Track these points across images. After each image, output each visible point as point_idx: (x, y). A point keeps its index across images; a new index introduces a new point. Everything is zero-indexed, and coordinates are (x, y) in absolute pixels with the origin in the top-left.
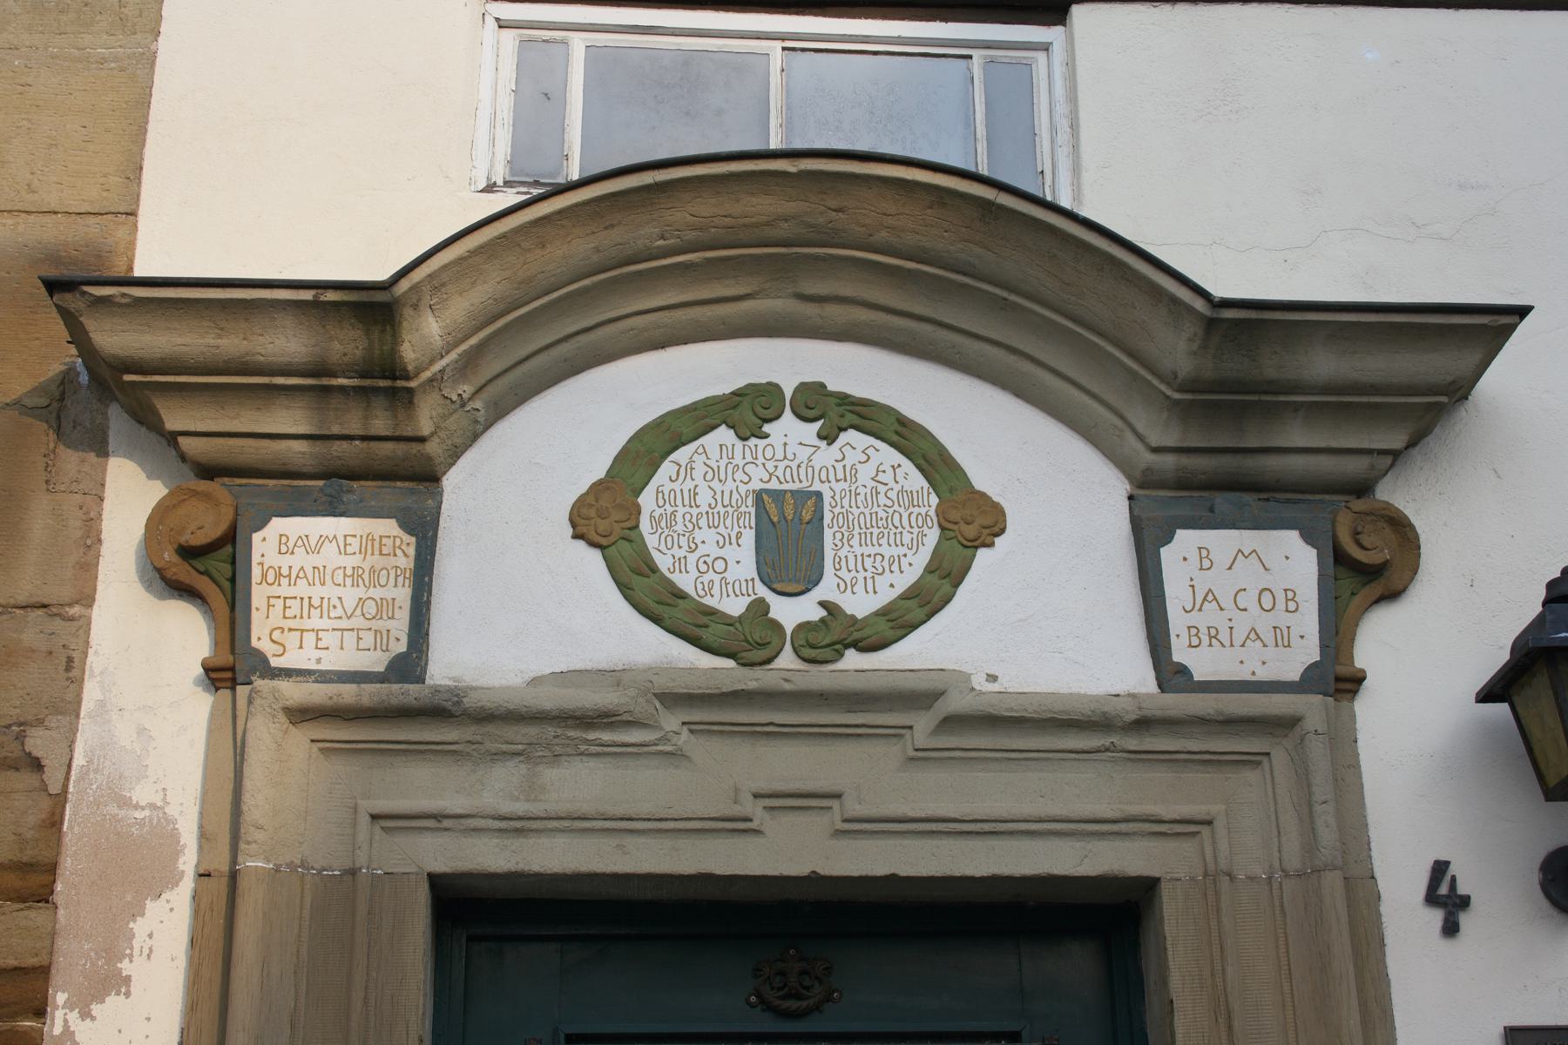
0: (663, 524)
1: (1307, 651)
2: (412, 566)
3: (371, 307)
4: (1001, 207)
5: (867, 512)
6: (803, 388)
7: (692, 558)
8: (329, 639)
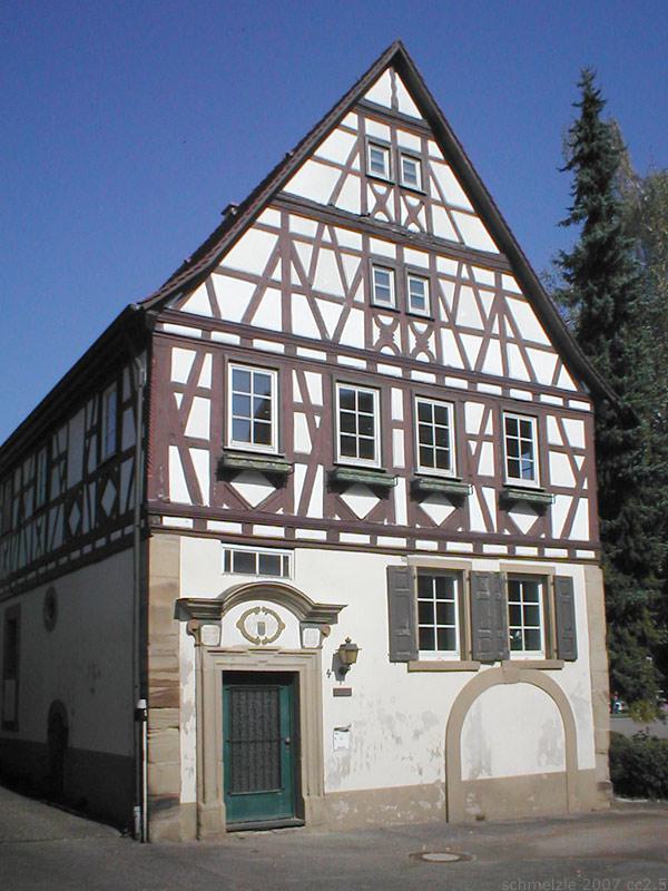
1: (318, 644)
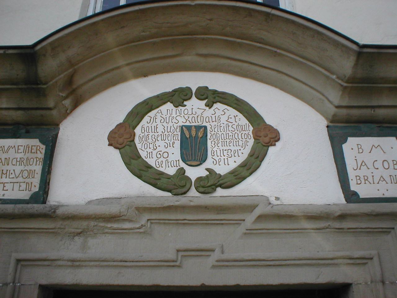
0: (144, 139)
2: (43, 157)
3: (28, 55)
4: (274, 15)
5: (224, 133)
6: (199, 89)
7: (154, 152)
8: (8, 186)
